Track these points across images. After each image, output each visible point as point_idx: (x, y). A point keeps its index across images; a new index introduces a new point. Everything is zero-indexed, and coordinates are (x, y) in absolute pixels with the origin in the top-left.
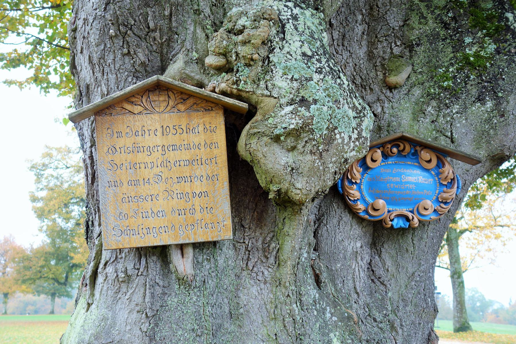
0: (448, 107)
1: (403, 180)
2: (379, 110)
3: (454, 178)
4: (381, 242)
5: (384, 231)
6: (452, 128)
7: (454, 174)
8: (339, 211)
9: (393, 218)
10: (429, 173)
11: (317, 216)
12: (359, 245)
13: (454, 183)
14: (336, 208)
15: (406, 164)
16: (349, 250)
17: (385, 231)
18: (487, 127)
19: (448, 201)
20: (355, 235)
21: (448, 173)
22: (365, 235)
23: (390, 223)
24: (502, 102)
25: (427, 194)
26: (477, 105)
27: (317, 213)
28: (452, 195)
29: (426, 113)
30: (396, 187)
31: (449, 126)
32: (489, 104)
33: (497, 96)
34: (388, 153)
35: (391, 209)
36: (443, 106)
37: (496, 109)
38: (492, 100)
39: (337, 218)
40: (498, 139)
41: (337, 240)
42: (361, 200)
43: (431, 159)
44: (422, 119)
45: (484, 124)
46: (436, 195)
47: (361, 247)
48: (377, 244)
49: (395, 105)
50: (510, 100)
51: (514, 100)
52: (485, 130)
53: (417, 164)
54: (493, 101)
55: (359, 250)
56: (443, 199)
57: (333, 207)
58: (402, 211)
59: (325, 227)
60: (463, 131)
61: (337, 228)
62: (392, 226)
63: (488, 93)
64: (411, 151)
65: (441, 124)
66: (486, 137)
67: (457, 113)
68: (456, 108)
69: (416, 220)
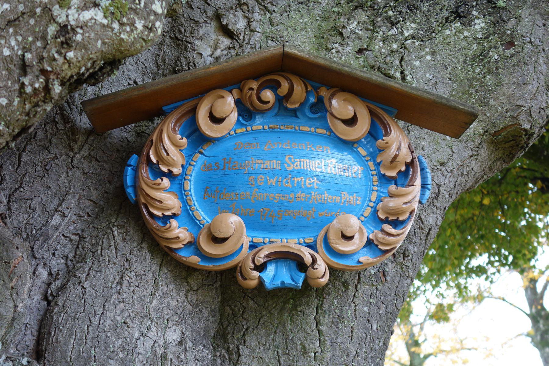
0: (393, 24)
1: (289, 165)
2: (241, 24)
3: (412, 162)
4: (239, 331)
5: (247, 301)
6: (404, 66)
7: (412, 152)
8: (125, 248)
9: (262, 261)
10: (353, 151)
11: (69, 263)
12: (173, 336)
13: (414, 173)
14: (119, 238)
15: (296, 132)
16: (141, 351)
17: (251, 303)
18: (478, 70)
19: (401, 218)
20: (166, 311)
21: (399, 149)
22: (196, 313)
23: (256, 274)
24: (505, 19)
25: (350, 203)
26: (453, 26)
27: (71, 256)
28: (409, 202)
29: (346, 33)
30: (269, 182)
31: (397, 62)
32: (479, 25)
33: (495, 7)
34: (252, 104)
35: (258, 240)
36: (383, 20)
37: (495, 33)
38: (484, 16)
39: (118, 265)
40: (504, 94)
41: (109, 322)
42: (183, 217)
43: (355, 114)
44: (337, 45)
45: (472, 65)
46: (372, 204)
47: (181, 343)
48: (229, 337)
49: (276, 17)
50: (523, 16)
51: (530, 17)
52: (474, 78)
53: (324, 131)
54: (487, 16)
55: (172, 349)
56: (389, 212)
57: (111, 237)
58: (287, 244)
59: (80, 288)
60: (427, 75)
61: (114, 291)
62: (261, 282)
63: (474, 3)
64: (307, 99)
65: (378, 54)
66: (477, 91)
67: (413, 38)
68: (410, 29)
69: (321, 267)
